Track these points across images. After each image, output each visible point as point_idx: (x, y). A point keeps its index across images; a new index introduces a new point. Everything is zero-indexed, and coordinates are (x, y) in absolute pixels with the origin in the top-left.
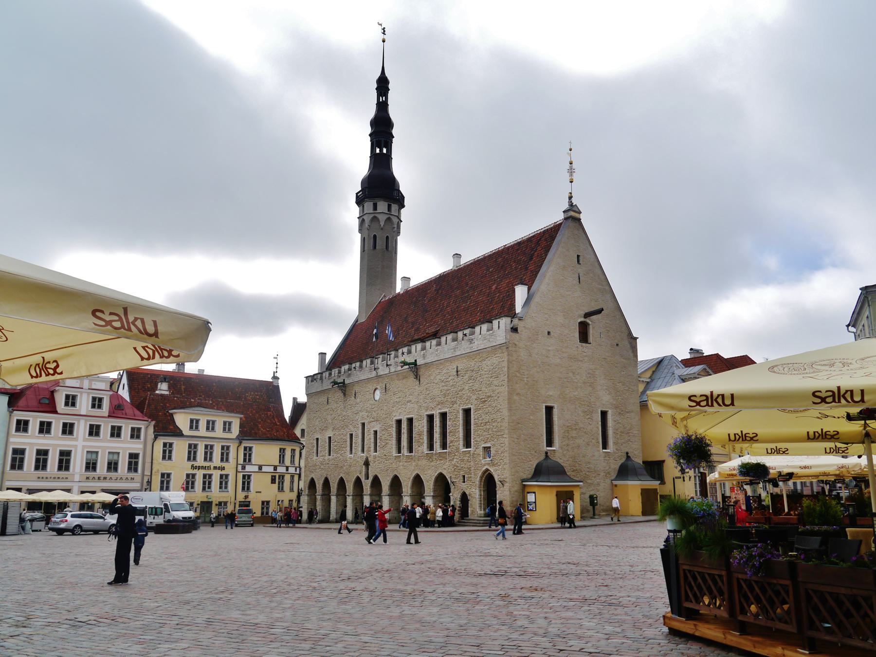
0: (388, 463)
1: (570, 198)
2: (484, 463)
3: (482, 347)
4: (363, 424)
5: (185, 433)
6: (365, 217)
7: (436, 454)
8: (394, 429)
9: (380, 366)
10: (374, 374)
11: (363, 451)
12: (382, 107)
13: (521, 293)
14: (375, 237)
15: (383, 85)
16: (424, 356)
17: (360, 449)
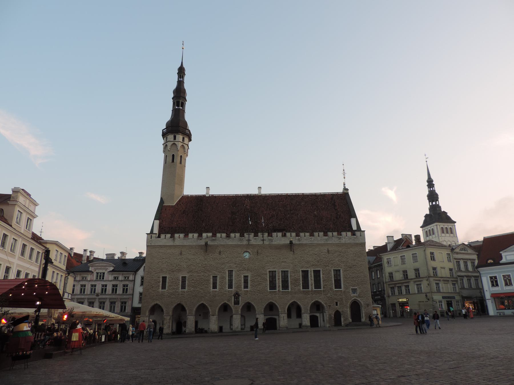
0: (259, 295)
1: (344, 184)
2: (354, 296)
3: (349, 242)
4: (231, 272)
5: (55, 263)
6: (176, 143)
7: (312, 291)
8: (268, 276)
9: (251, 239)
10: (245, 243)
11: (230, 286)
12: (180, 83)
13: (353, 221)
14: (181, 156)
15: (181, 72)
16: (299, 240)
17: (227, 286)
